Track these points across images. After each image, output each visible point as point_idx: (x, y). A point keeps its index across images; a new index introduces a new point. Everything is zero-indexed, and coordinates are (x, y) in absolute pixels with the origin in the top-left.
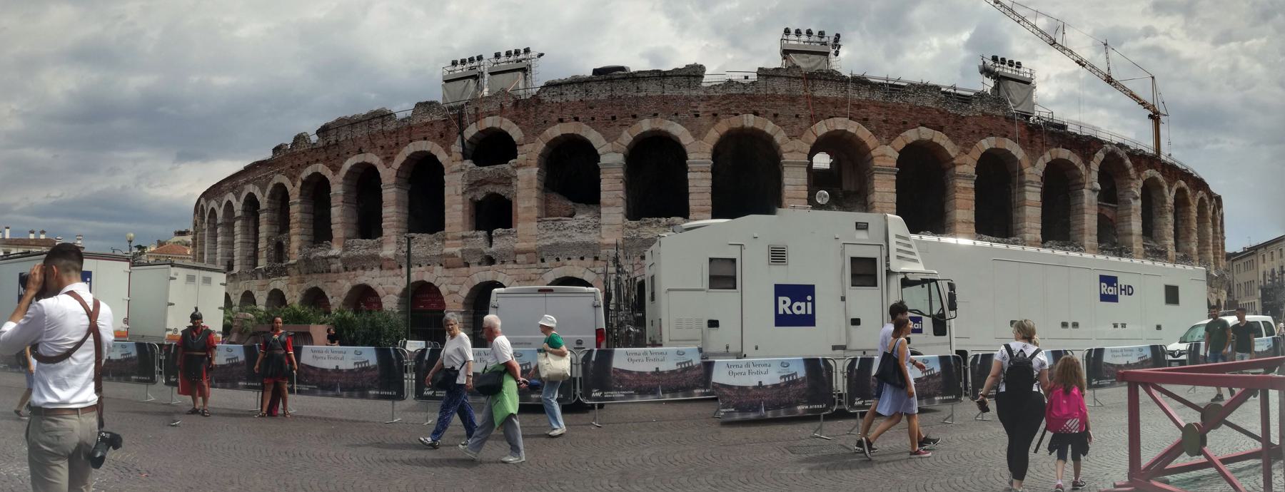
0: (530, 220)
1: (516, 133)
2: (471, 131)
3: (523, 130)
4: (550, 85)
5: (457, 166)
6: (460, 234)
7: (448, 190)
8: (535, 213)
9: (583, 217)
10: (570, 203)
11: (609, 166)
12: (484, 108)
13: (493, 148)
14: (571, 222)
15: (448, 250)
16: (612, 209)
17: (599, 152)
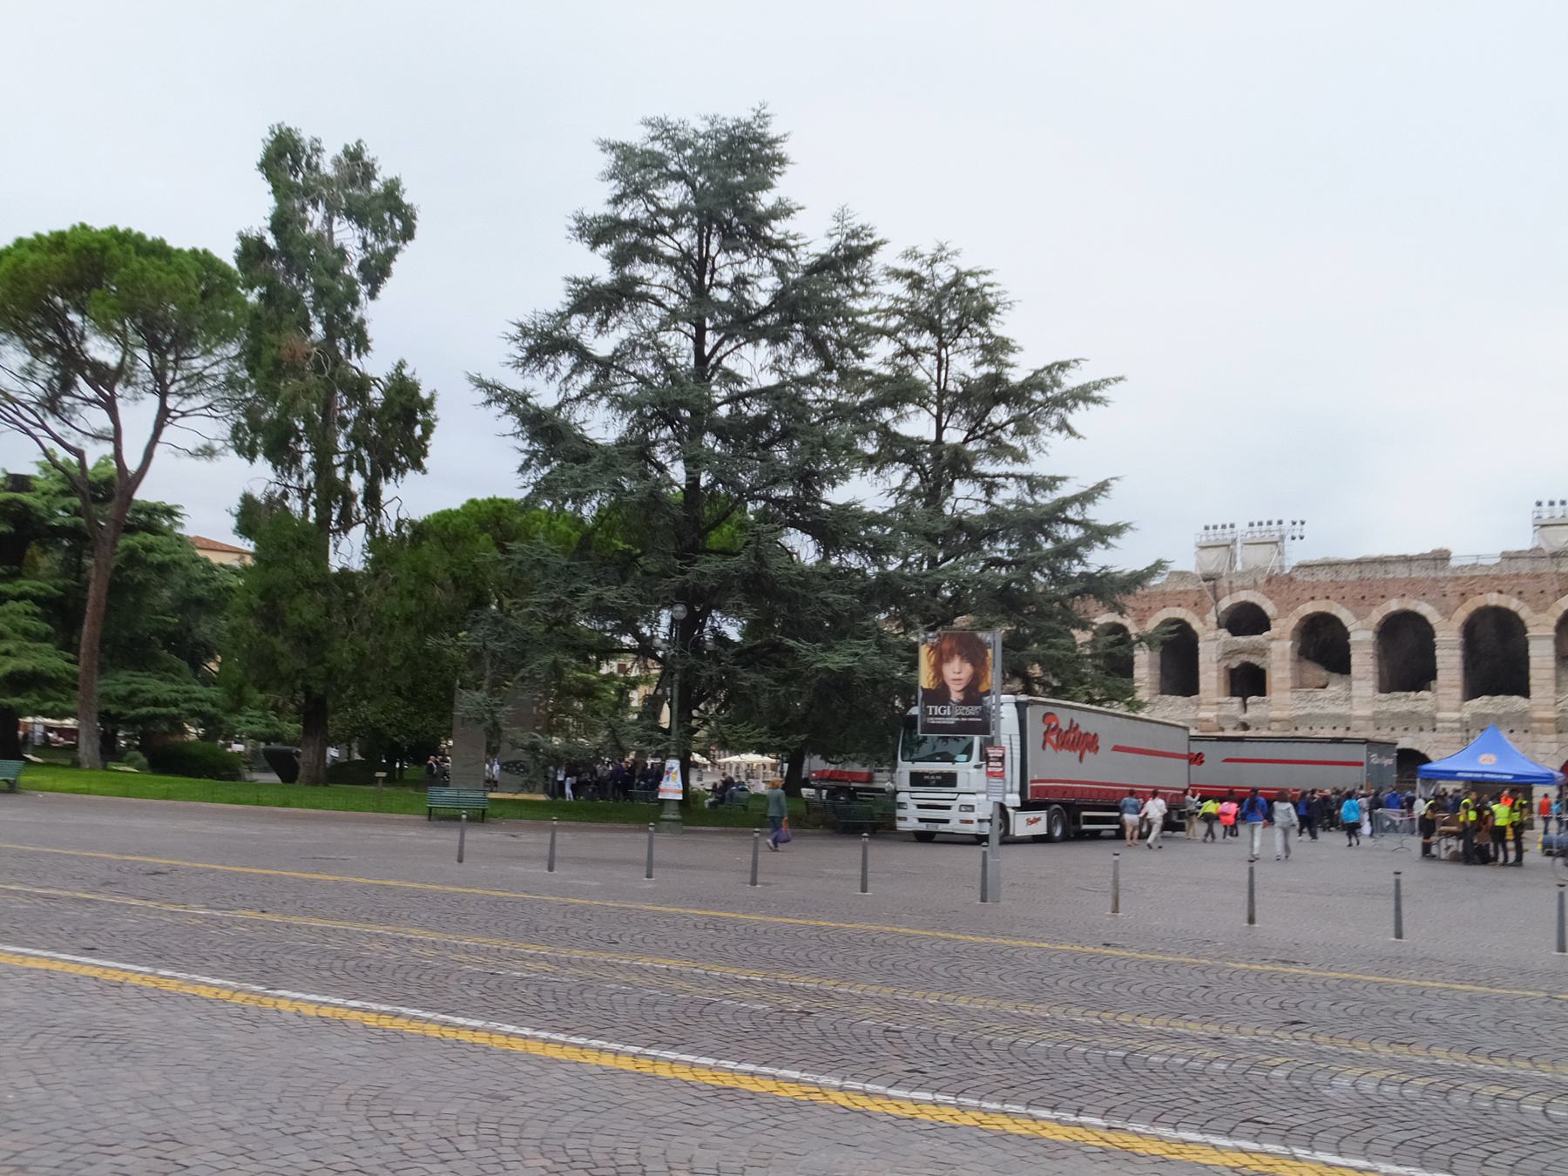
0: (1285, 690)
1: (1269, 608)
2: (1225, 603)
3: (1277, 605)
4: (1301, 566)
5: (1212, 635)
6: (1216, 700)
7: (1202, 658)
8: (1289, 684)
9: (1335, 688)
10: (1325, 673)
11: (1359, 643)
12: (1238, 583)
13: (1247, 620)
14: (1322, 694)
15: (1203, 715)
16: (1363, 683)
17: (1350, 629)
